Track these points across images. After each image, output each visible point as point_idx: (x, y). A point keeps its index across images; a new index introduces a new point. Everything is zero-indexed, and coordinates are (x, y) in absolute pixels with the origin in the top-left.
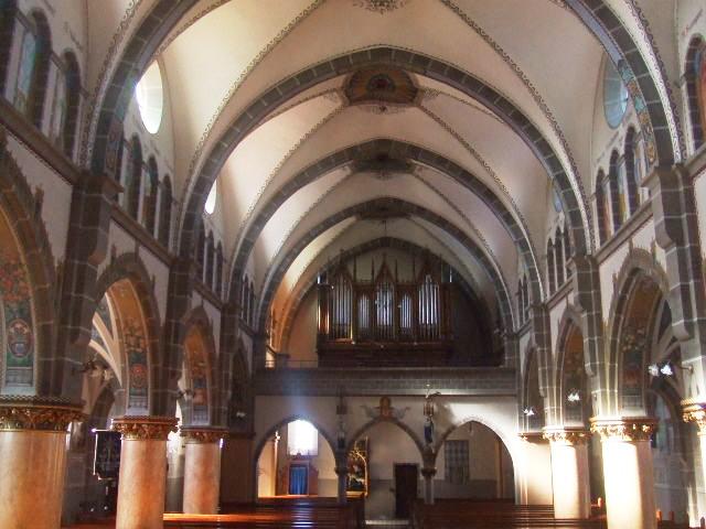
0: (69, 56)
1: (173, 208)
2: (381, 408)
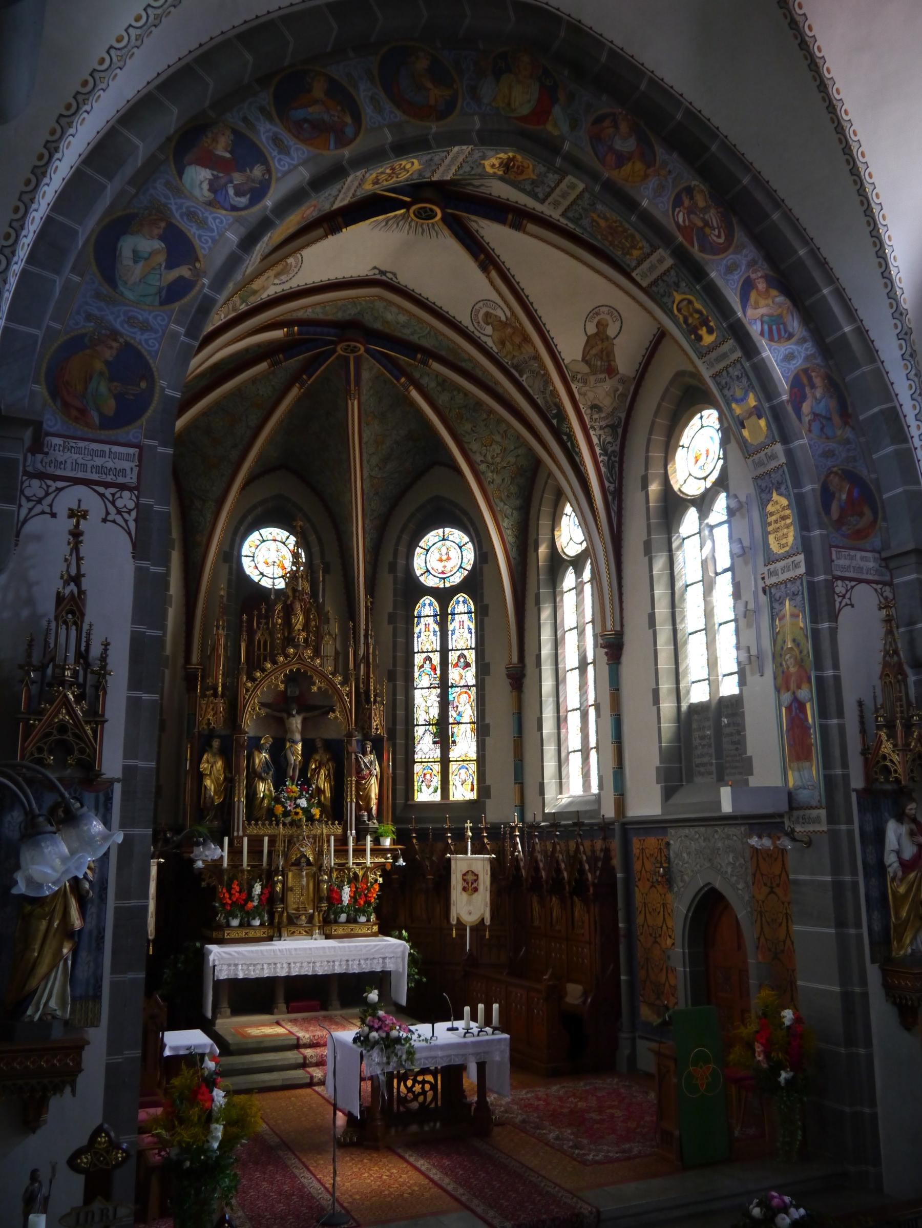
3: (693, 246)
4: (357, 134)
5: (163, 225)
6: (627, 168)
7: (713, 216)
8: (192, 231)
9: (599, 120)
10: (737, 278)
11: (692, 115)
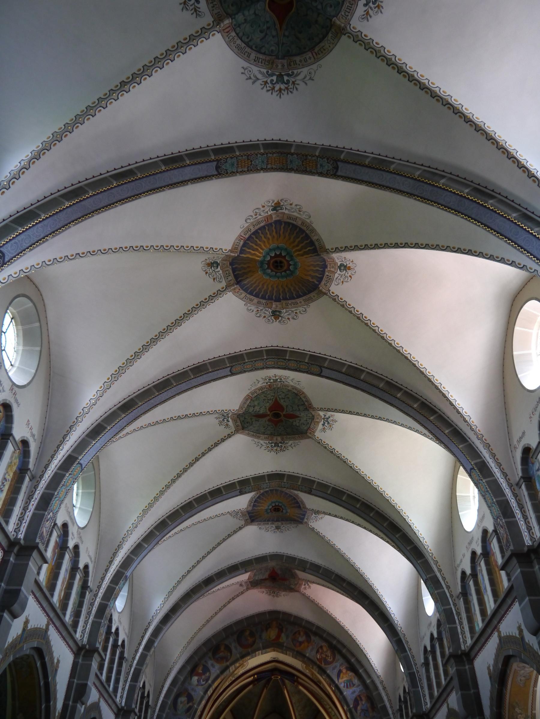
0: (25, 443)
1: (88, 595)
3: (322, 664)
4: (231, 657)
5: (187, 693)
6: (303, 645)
7: (329, 653)
8: (193, 693)
9: (295, 633)
10: (336, 671)
11: (318, 627)
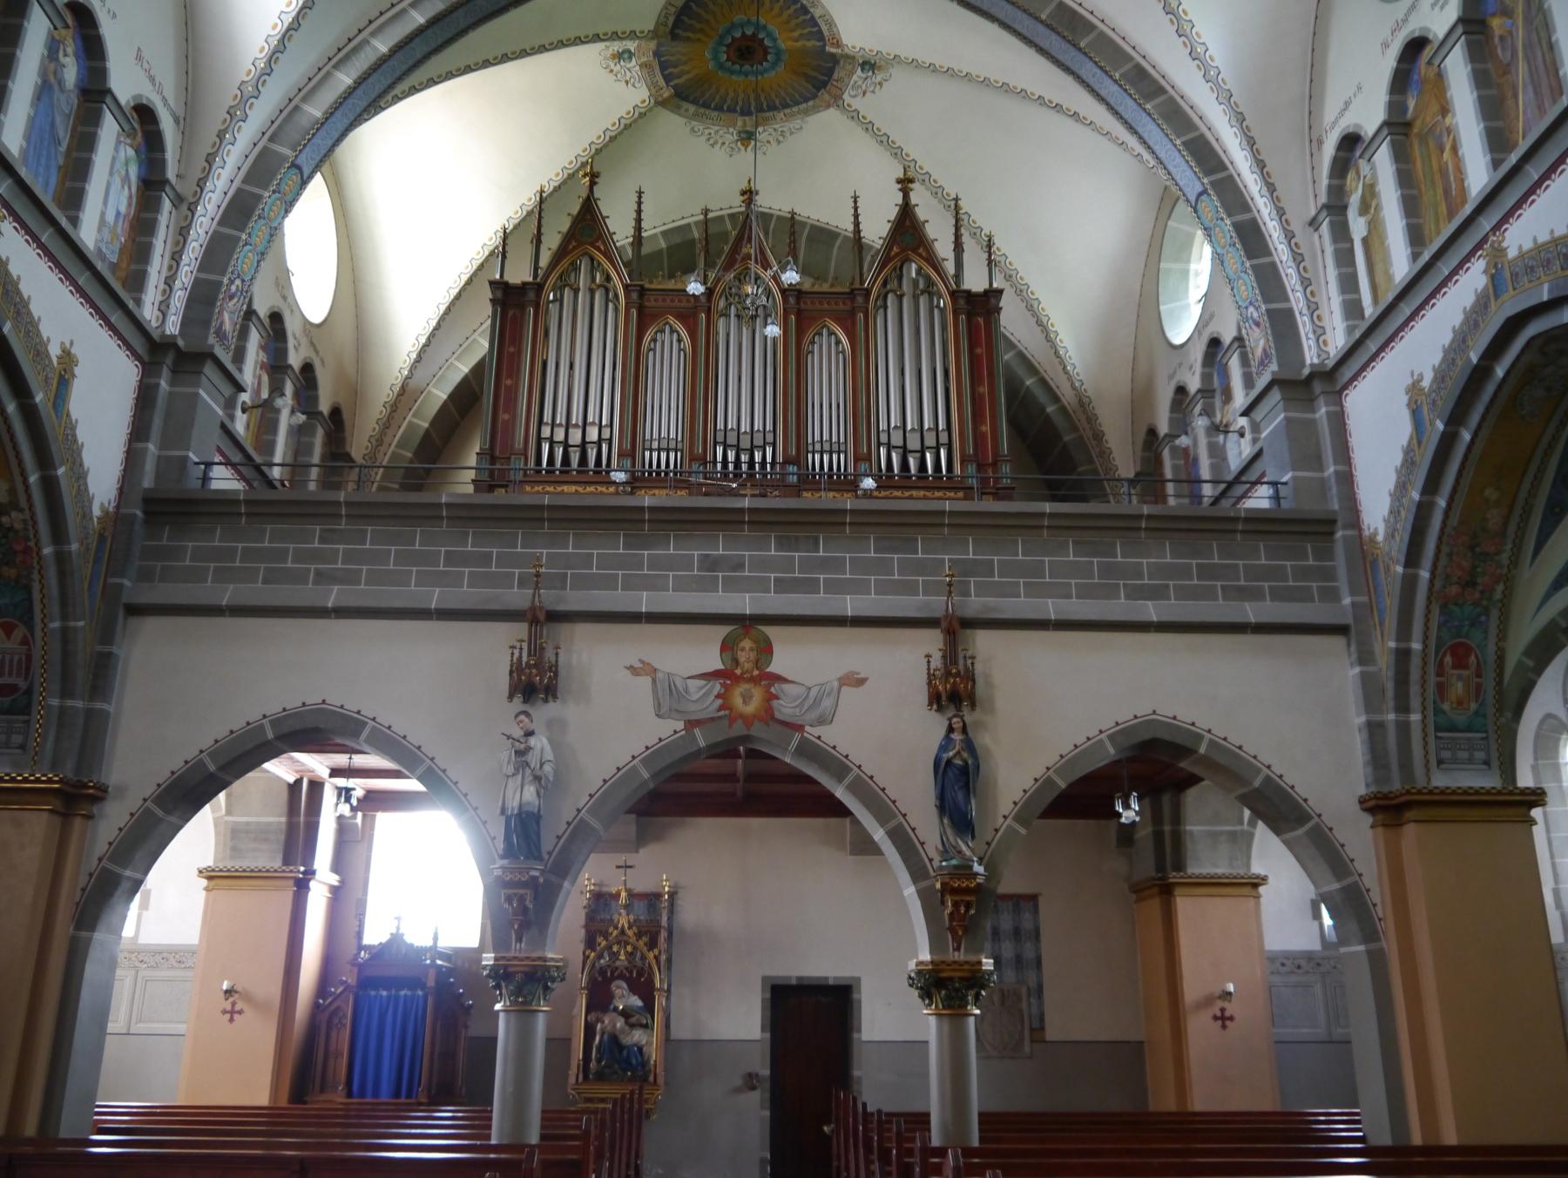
2: (725, 676)
